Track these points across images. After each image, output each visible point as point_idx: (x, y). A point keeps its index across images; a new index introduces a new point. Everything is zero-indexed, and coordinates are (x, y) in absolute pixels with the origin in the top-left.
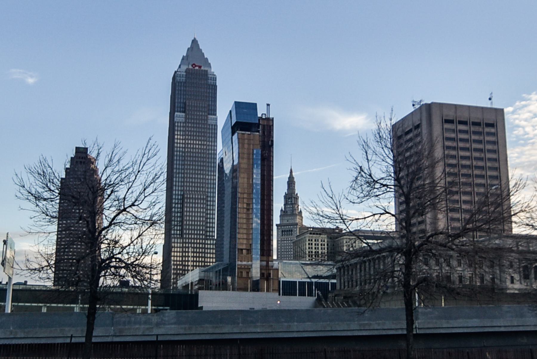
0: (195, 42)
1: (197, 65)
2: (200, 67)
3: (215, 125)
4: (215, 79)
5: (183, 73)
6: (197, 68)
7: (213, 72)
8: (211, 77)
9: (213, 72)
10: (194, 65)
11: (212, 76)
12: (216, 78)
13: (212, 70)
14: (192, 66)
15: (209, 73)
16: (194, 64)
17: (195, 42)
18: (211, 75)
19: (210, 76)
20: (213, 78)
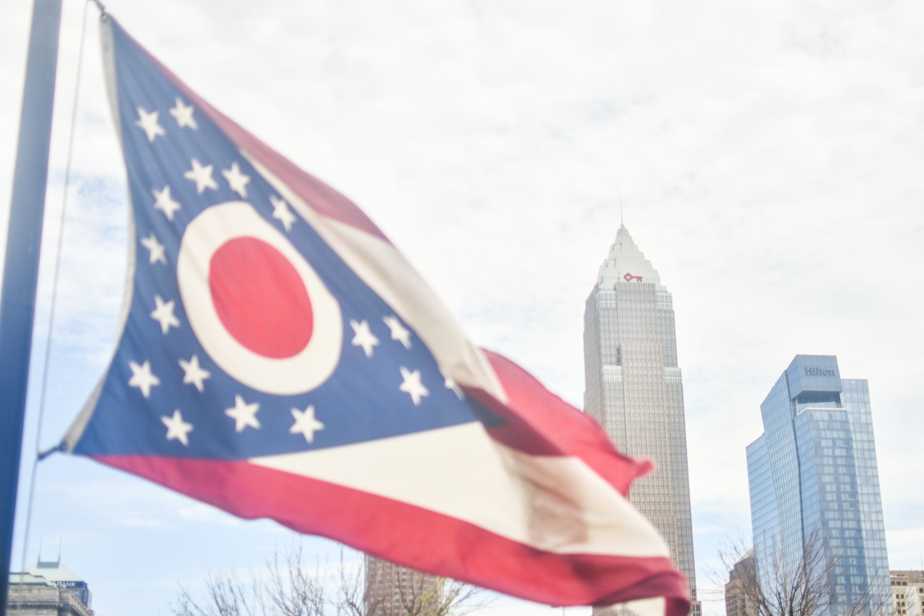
0: (622, 232)
1: (633, 275)
2: (640, 279)
3: (677, 385)
4: (669, 299)
5: (609, 292)
6: (634, 281)
7: (665, 287)
8: (662, 297)
9: (665, 287)
10: (628, 277)
11: (664, 294)
12: (671, 297)
13: (663, 283)
14: (625, 277)
15: (657, 288)
16: (628, 274)
17: (622, 232)
18: (660, 291)
19: (660, 294)
20: (667, 297)
